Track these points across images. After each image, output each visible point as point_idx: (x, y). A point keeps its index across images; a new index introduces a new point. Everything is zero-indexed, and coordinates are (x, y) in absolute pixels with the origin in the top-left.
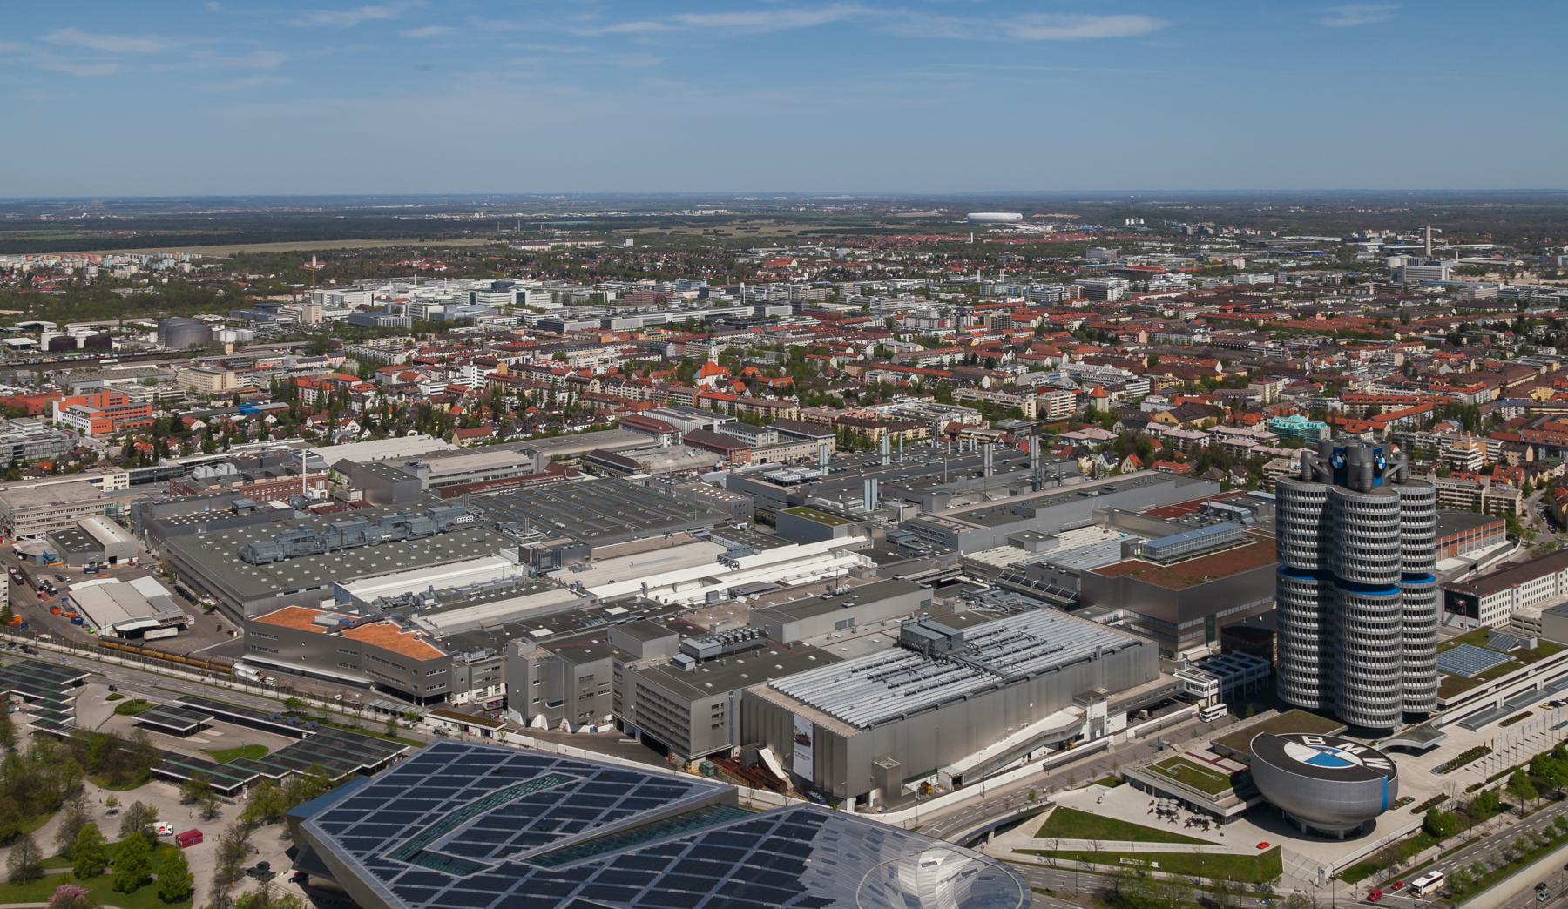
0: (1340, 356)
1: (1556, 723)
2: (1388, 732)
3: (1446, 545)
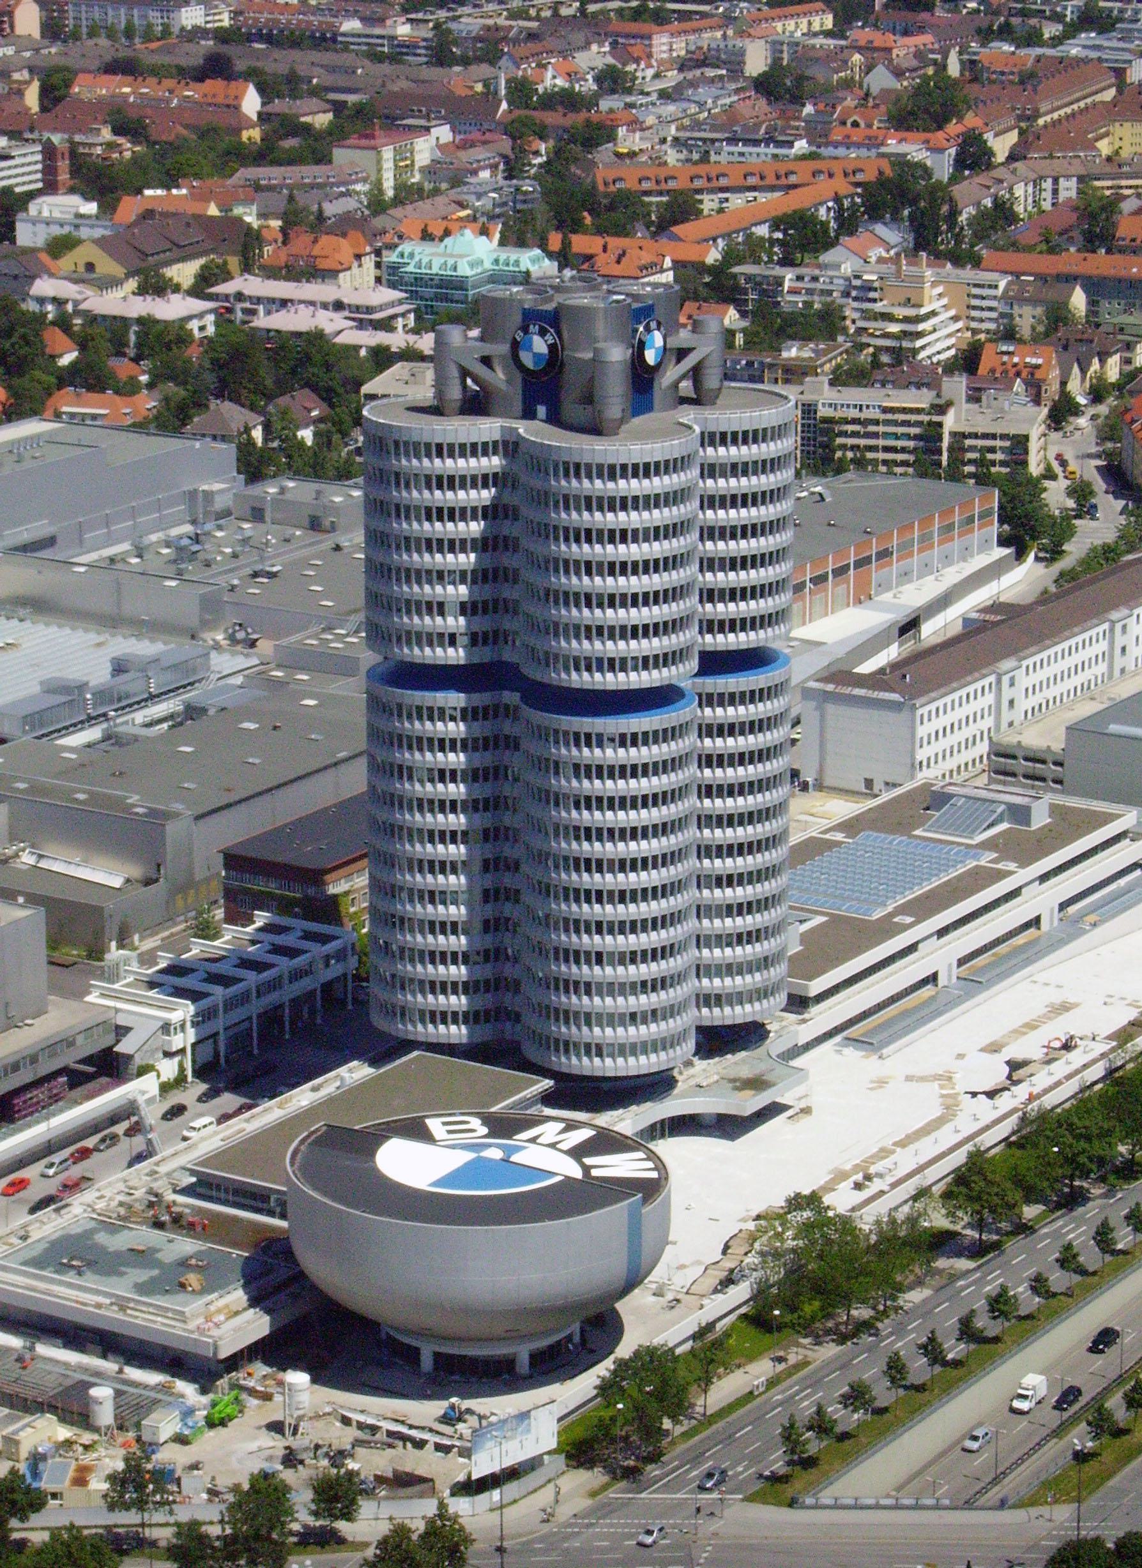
0: (595, 57)
2: (658, 1085)
3: (840, 572)
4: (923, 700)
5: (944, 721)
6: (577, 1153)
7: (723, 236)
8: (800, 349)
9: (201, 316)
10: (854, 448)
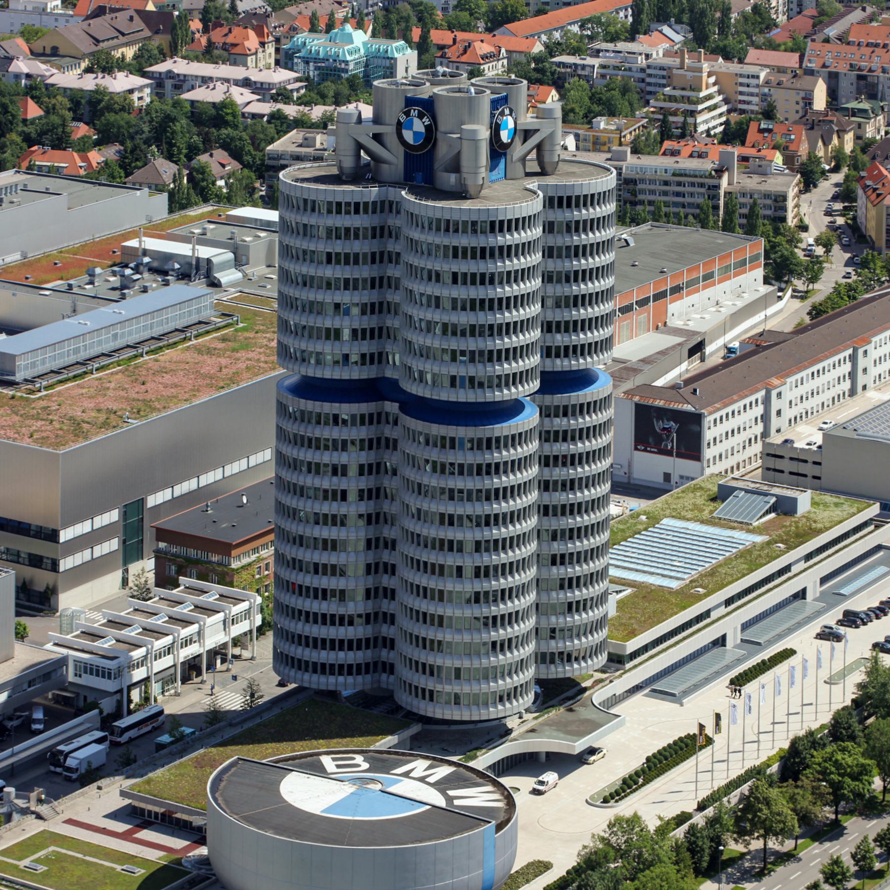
1: (838, 666)
3: (643, 303)
4: (710, 409)
5: (727, 426)
6: (442, 786)
7: (545, 33)
8: (608, 124)
9: (141, 89)
10: (651, 203)
